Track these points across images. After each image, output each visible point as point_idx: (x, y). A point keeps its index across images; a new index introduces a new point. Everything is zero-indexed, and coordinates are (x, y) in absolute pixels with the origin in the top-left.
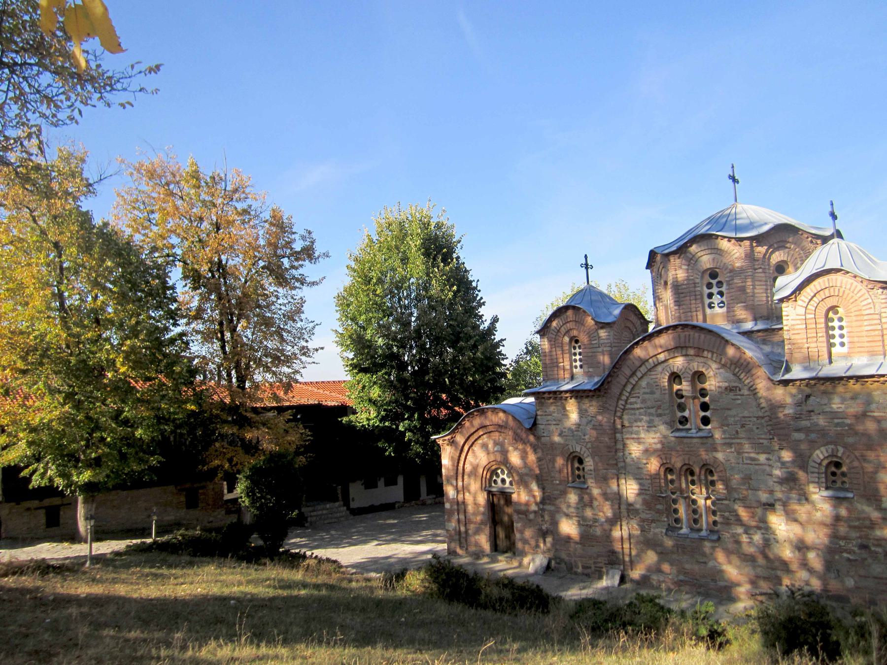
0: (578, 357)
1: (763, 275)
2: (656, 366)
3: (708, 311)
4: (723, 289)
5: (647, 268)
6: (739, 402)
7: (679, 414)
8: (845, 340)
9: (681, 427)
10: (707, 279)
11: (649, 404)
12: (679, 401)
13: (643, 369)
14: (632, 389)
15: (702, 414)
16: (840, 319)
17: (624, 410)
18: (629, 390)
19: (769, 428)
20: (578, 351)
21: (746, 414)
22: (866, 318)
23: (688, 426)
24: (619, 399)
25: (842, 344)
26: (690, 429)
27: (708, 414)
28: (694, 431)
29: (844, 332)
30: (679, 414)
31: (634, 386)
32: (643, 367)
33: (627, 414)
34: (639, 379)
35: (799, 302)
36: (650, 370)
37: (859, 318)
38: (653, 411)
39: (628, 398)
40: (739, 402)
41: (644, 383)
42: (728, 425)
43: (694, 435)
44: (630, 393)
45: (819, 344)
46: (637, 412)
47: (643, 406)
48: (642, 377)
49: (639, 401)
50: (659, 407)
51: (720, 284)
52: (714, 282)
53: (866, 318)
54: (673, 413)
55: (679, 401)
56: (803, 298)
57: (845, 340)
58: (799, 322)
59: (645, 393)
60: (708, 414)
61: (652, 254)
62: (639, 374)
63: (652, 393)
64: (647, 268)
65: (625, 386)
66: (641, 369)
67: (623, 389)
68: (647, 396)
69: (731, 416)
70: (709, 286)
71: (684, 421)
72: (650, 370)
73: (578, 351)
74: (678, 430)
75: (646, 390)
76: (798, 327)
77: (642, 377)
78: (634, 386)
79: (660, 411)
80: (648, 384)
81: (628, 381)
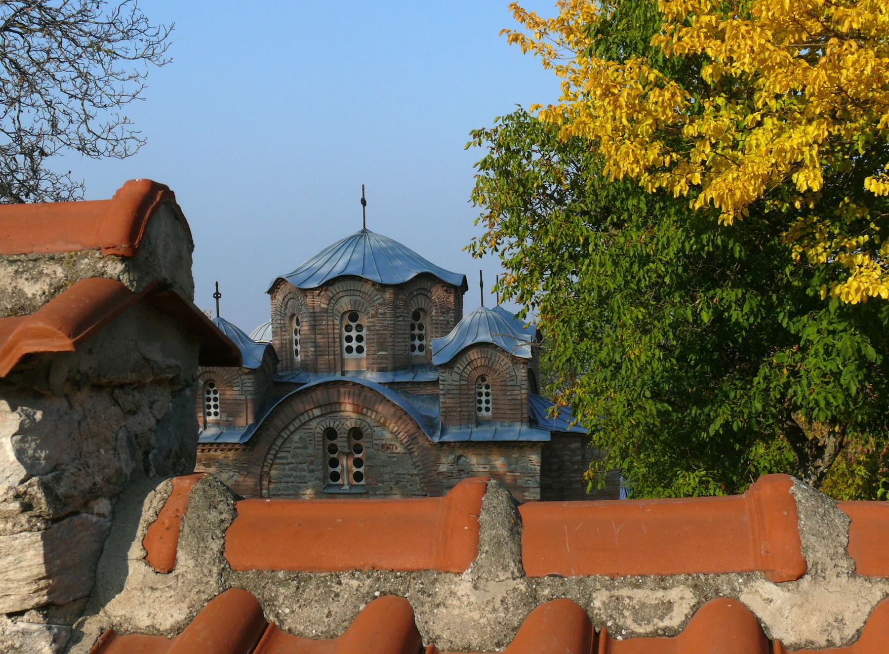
0: (212, 403)
1: (403, 323)
2: (310, 420)
3: (346, 355)
4: (364, 333)
5: (269, 292)
6: (395, 459)
7: (332, 470)
8: (490, 405)
9: (333, 483)
10: (346, 321)
11: (301, 459)
12: (332, 456)
13: (297, 423)
14: (283, 443)
15: (355, 470)
16: (487, 387)
17: (272, 464)
18: (279, 444)
19: (423, 485)
20: (212, 396)
21: (401, 471)
22: (509, 388)
23: (340, 482)
24: (268, 453)
25: (487, 409)
26: (343, 485)
27: (361, 470)
28: (346, 487)
29: (490, 398)
30: (332, 470)
31: (285, 440)
32: (297, 420)
33: (276, 469)
34: (291, 433)
35: (456, 369)
36: (304, 424)
37: (504, 388)
38: (305, 466)
39: (277, 452)
40: (395, 459)
41: (296, 437)
42: (382, 482)
43: (348, 491)
44: (280, 447)
45: (470, 409)
46: (287, 467)
47: (293, 461)
48: (294, 431)
49: (289, 455)
50: (312, 463)
51: (359, 328)
52: (353, 325)
53: (509, 388)
54: (325, 469)
55: (332, 456)
56: (458, 365)
57: (490, 405)
58: (454, 387)
59: (296, 448)
60: (361, 470)
61: (279, 283)
62: (292, 428)
63: (305, 448)
64: (269, 292)
65: (275, 440)
66: (295, 423)
67: (273, 443)
68: (298, 451)
69: (386, 473)
70: (348, 328)
71: (336, 476)
72: (304, 424)
73: (212, 396)
74: (330, 486)
75: (299, 445)
76: (455, 392)
77: (294, 431)
78: (285, 440)
79: (312, 467)
80: (301, 438)
81: (279, 435)
